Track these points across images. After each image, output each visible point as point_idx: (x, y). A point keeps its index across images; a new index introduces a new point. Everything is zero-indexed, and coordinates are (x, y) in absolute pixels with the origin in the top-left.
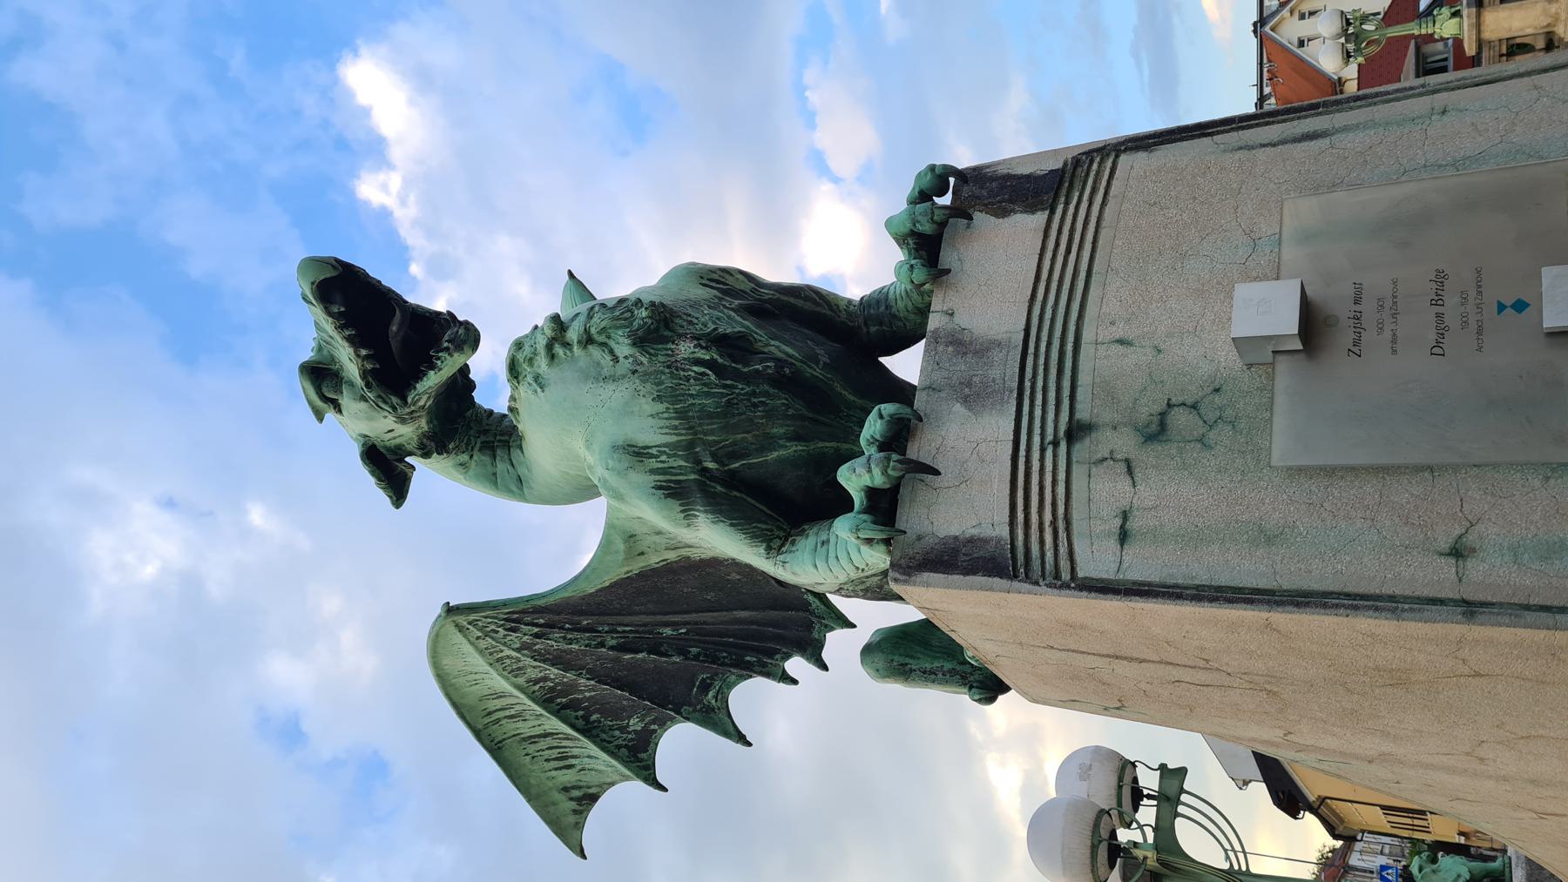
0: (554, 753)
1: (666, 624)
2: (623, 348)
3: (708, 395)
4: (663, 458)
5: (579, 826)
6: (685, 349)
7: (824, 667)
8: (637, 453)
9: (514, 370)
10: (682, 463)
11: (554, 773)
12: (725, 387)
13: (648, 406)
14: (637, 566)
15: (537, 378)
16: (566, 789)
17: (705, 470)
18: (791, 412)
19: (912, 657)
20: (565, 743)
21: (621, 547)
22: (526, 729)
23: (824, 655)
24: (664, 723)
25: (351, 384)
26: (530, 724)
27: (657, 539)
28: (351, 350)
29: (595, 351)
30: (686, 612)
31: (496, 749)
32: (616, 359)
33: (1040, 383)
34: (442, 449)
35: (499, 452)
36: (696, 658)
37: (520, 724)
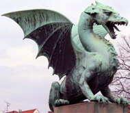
2: (114, 64)
5: (10, 17)
6: (112, 72)
8: (101, 65)
13: (107, 67)
14: (75, 52)
22: (37, 17)
24: (39, 43)
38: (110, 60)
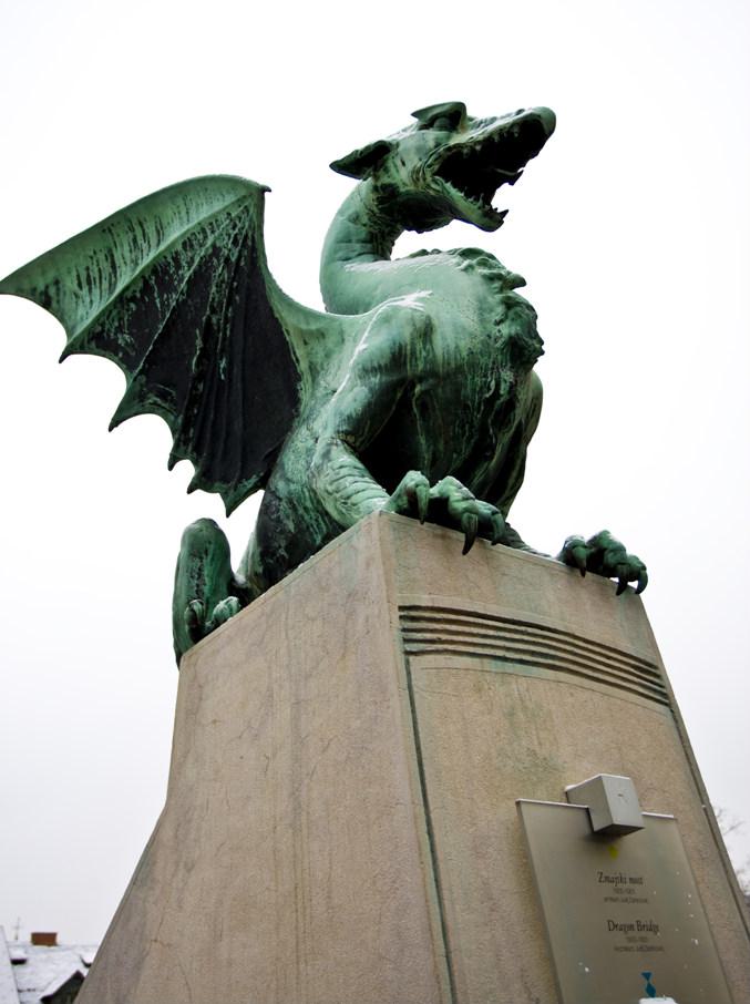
0: (94, 274)
1: (230, 363)
2: (506, 330)
3: (474, 390)
4: (424, 354)
5: (19, 292)
6: (507, 375)
7: (190, 490)
8: (426, 331)
9: (468, 253)
10: (421, 366)
11: (74, 273)
12: (479, 404)
13: (465, 344)
14: (293, 340)
15: (470, 267)
16: (57, 282)
17: (414, 387)
18: (455, 456)
19: (212, 559)
20: (105, 284)
21: (313, 327)
22: (123, 252)
23: (199, 493)
24: (127, 364)
25: (449, 138)
26: (127, 254)
27: (321, 354)
28: (481, 138)
29: (500, 309)
30: (243, 380)
31: (106, 228)
32: (498, 323)
33: (526, 638)
34: (380, 201)
35: (369, 246)
36: (195, 388)
37: (126, 248)
38: (483, 309)
